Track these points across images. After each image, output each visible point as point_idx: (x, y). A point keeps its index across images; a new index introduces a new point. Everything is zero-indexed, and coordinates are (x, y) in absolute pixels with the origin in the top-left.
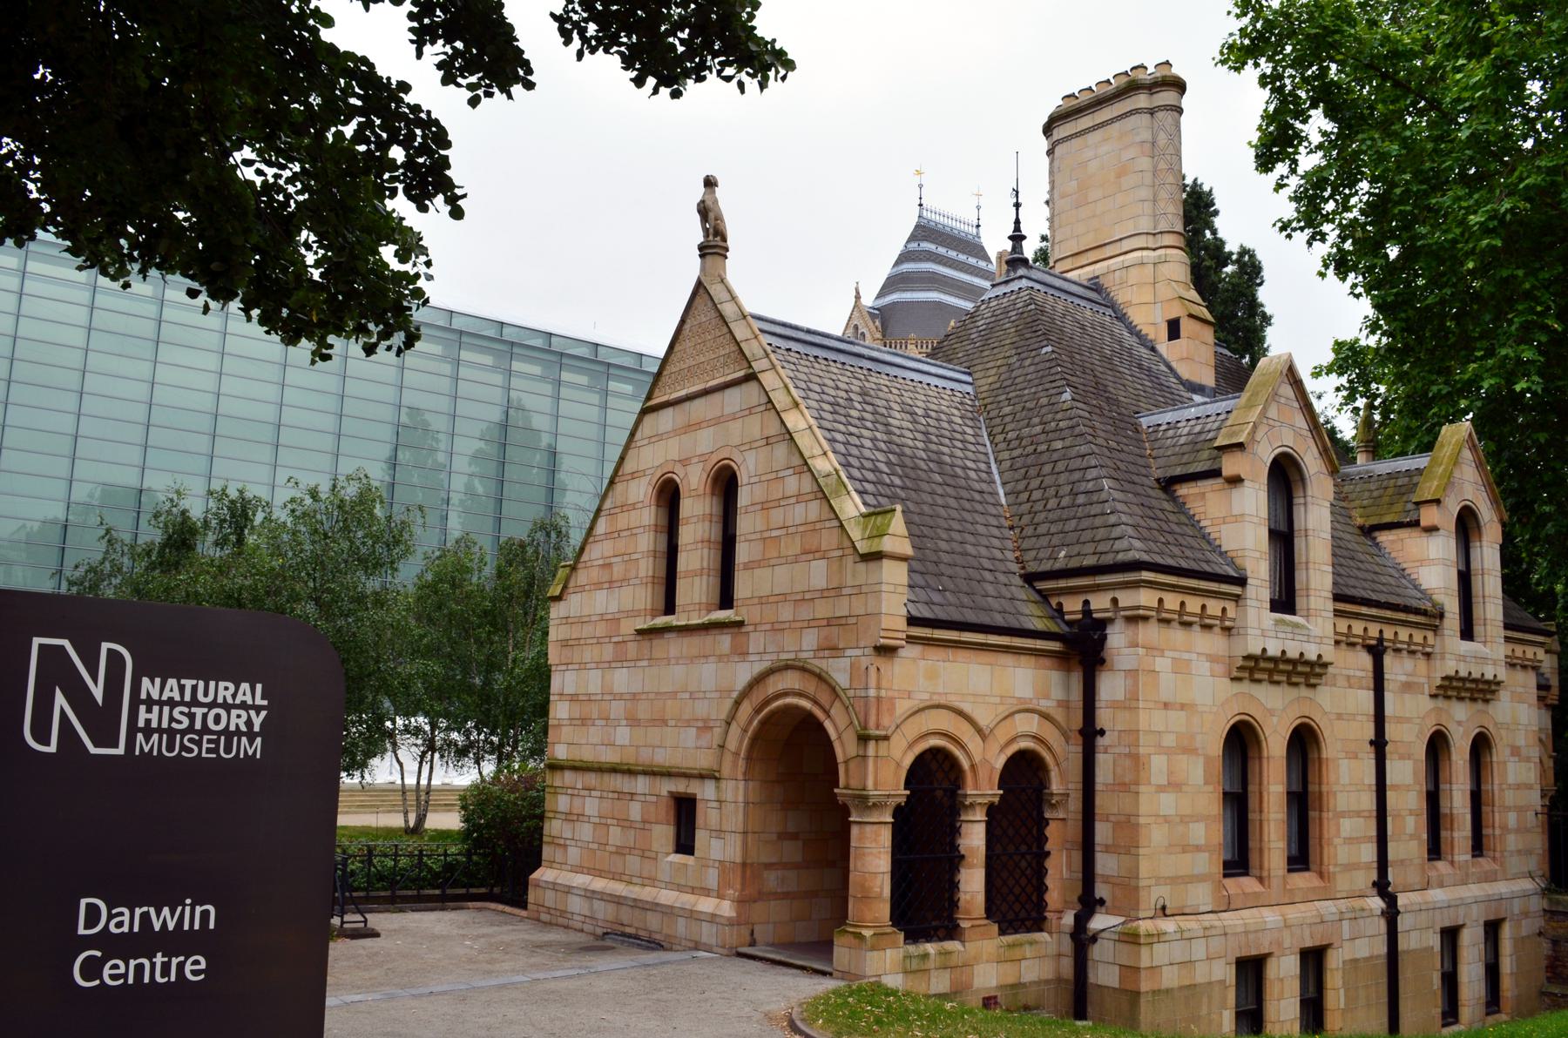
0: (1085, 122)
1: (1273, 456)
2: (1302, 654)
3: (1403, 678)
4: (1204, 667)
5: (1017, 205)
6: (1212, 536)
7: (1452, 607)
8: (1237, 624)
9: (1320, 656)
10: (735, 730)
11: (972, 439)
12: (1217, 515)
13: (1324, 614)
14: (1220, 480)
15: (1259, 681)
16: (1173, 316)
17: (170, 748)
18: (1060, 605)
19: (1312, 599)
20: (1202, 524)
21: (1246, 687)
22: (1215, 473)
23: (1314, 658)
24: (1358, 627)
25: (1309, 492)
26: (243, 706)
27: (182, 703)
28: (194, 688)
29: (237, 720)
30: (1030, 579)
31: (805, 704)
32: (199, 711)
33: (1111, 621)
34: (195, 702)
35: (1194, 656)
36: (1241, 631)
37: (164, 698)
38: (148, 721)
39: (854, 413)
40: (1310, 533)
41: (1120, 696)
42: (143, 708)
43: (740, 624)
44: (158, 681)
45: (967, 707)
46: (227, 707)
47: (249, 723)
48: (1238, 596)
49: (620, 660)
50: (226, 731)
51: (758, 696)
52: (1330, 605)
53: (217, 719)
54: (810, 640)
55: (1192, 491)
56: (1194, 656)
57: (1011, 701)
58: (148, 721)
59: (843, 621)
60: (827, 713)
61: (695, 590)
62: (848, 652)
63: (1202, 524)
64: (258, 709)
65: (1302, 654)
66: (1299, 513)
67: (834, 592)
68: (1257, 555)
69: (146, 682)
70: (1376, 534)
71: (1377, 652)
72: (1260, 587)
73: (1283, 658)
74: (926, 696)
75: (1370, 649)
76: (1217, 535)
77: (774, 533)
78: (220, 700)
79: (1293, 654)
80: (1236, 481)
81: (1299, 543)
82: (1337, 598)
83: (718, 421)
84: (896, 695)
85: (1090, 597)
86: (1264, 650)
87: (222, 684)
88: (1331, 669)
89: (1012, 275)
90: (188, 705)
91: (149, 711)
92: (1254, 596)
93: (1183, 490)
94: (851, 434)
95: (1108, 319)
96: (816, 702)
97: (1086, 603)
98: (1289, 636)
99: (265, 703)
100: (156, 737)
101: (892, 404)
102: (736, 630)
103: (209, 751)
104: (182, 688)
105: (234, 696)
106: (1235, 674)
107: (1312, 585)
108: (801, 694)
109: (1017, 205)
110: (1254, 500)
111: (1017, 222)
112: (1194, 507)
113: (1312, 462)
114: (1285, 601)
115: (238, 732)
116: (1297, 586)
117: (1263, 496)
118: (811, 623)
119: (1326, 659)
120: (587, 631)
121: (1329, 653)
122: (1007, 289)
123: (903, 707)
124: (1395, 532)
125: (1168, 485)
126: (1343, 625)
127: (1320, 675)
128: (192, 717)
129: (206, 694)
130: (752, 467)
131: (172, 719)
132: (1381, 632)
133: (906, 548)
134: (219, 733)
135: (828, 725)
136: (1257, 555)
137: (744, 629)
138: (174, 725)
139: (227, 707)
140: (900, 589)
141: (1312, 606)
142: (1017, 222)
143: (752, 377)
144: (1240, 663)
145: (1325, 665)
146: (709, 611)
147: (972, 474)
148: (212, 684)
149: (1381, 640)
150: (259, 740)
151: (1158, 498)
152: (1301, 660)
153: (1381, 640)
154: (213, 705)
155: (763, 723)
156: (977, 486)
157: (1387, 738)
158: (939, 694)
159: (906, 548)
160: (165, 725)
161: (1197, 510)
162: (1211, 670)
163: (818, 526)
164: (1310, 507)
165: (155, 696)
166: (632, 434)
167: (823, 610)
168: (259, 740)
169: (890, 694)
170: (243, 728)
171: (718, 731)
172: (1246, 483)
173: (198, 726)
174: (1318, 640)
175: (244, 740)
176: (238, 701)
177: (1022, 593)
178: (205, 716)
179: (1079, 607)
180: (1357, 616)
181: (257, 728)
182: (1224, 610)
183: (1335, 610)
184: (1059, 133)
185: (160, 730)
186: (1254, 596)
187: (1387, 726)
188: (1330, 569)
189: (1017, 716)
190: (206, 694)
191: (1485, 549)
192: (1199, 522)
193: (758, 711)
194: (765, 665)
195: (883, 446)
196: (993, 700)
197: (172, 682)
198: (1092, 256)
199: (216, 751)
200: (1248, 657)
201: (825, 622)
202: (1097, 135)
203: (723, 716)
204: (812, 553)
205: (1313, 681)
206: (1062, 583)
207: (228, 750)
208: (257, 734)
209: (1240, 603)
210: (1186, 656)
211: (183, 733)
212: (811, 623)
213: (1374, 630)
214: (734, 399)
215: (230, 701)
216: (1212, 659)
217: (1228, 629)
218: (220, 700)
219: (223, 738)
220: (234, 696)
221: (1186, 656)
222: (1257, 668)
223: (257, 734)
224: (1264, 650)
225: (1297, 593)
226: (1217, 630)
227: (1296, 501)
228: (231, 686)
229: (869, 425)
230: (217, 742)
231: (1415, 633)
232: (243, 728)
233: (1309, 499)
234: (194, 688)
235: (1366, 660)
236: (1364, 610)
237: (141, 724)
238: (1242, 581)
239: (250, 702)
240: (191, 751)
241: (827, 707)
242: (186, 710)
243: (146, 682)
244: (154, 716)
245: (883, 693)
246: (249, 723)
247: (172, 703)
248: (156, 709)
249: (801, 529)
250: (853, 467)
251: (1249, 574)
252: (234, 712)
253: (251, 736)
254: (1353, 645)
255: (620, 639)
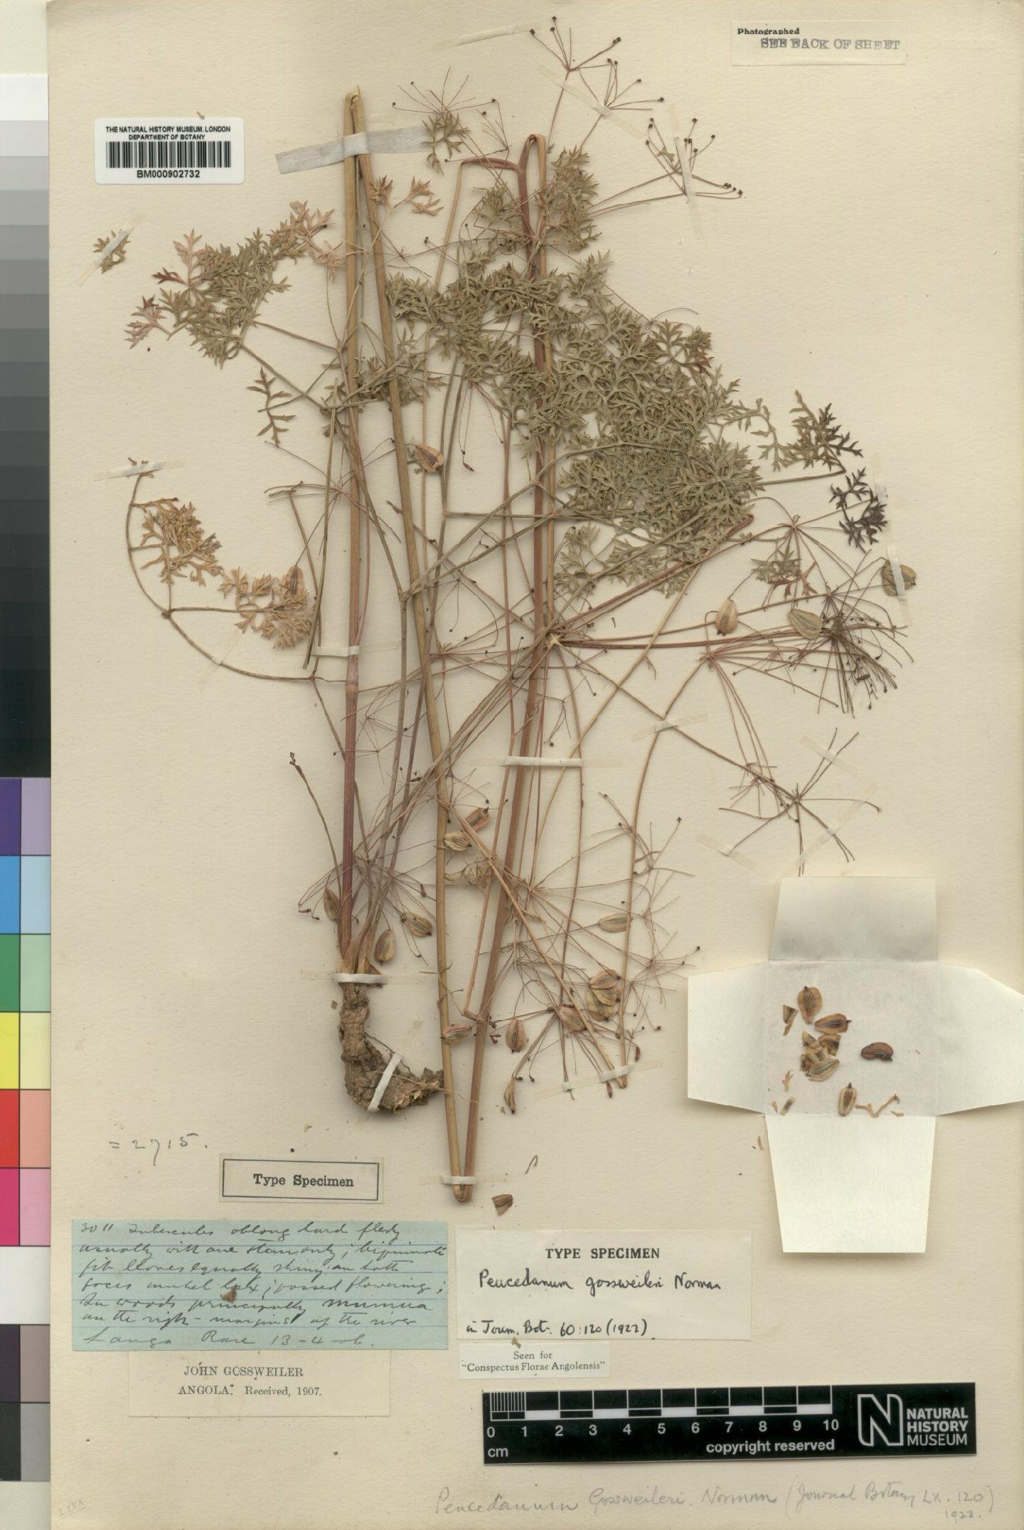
17: (924, 1442)
26: (956, 1419)
27: (927, 1420)
28: (932, 1413)
29: (953, 1426)
32: (935, 1423)
34: (933, 1419)
37: (919, 1418)
38: (912, 1430)
42: (909, 1424)
44: (915, 1410)
46: (948, 1420)
47: (959, 1427)
50: (949, 1432)
53: (944, 1426)
58: (912, 1430)
64: (963, 1420)
69: (909, 1411)
78: (944, 1417)
87: (945, 1409)
90: (930, 1420)
91: (912, 1425)
99: (967, 1417)
100: (916, 1436)
103: (942, 1442)
104: (926, 1413)
105: (951, 1414)
115: (955, 1432)
128: (932, 1426)
129: (938, 1415)
131: (923, 1428)
134: (946, 1433)
138: (924, 1430)
139: (948, 1420)
148: (940, 1409)
150: (965, 1436)
154: (941, 1419)
160: (920, 1430)
165: (914, 1417)
168: (965, 1436)
170: (957, 1430)
173: (936, 1430)
175: (958, 1435)
176: (953, 1417)
178: (938, 1425)
181: (964, 1429)
185: (918, 1433)
190: (938, 1415)
197: (921, 1410)
199: (945, 1442)
207: (951, 1440)
208: (964, 1432)
211: (929, 1434)
215: (949, 1417)
218: (944, 1417)
219: (948, 1436)
220: (951, 1414)
223: (964, 1432)
228: (949, 1410)
230: (945, 1437)
232: (957, 1430)
234: (932, 1413)
237: (909, 1431)
239: (959, 1417)
240: (933, 1442)
242: (929, 1423)
243: (909, 1411)
244: (915, 1427)
246: (959, 1427)
247: (922, 1420)
248: (915, 1423)
252: (952, 1423)
253: (961, 1434)
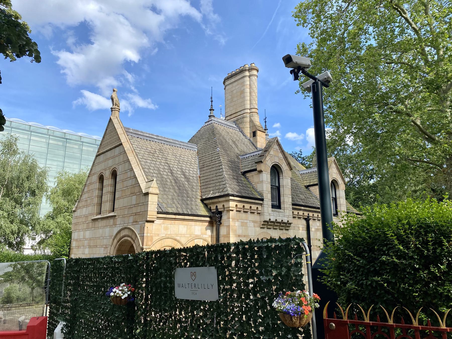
0: (233, 80)
1: (272, 165)
2: (282, 220)
3: (317, 227)
4: (252, 224)
5: (212, 101)
6: (255, 187)
7: (267, 196)
8: (262, 212)
9: (288, 221)
10: (113, 247)
11: (194, 163)
12: (256, 181)
13: (289, 209)
14: (257, 172)
15: (270, 228)
16: (254, 130)
18: (210, 207)
19: (285, 205)
20: (253, 184)
21: (265, 230)
22: (255, 170)
23: (286, 221)
24: (301, 213)
25: (284, 175)
30: (202, 200)
31: (129, 239)
33: (223, 211)
35: (248, 221)
36: (263, 214)
39: (156, 155)
40: (284, 186)
41: (225, 234)
43: (115, 216)
45: (178, 238)
48: (262, 204)
49: (88, 229)
51: (118, 237)
52: (291, 207)
54: (131, 219)
55: (250, 175)
56: (248, 221)
57: (193, 236)
59: (139, 213)
60: (134, 241)
61: (107, 206)
62: (140, 223)
63: (253, 184)
65: (282, 220)
66: (281, 180)
67: (137, 205)
68: (267, 192)
70: (309, 188)
71: (307, 220)
72: (268, 201)
73: (276, 221)
74: (164, 235)
75: (305, 219)
76: (256, 187)
77: (124, 189)
79: (279, 220)
80: (261, 172)
81: (281, 189)
82: (293, 205)
83: (113, 157)
84: (154, 235)
85: (218, 205)
86: (270, 219)
88: (292, 225)
89: (210, 120)
92: (266, 204)
93: (248, 175)
94: (153, 161)
95: (237, 132)
96: (132, 239)
97: (217, 206)
98: (278, 215)
101: (169, 153)
102: (114, 218)
106: (261, 226)
107: (285, 201)
108: (128, 236)
109: (212, 101)
110: (266, 177)
111: (212, 106)
112: (251, 179)
113: (284, 167)
114: (277, 206)
116: (281, 201)
117: (269, 176)
118: (132, 215)
119: (290, 222)
120: (80, 220)
121: (291, 220)
122: (208, 123)
123: (155, 238)
124: (314, 187)
125: (244, 173)
126: (296, 212)
127: (289, 227)
130: (120, 170)
132: (308, 214)
133: (157, 191)
135: (134, 245)
136: (267, 192)
137: (116, 217)
140: (155, 203)
141: (285, 207)
142: (212, 106)
143: (121, 144)
144: (263, 223)
145: (290, 224)
146: (109, 213)
147: (191, 172)
149: (308, 217)
151: (243, 178)
152: (282, 222)
153: (308, 217)
155: (120, 245)
156: (192, 175)
157: (311, 244)
158: (169, 234)
159: (157, 191)
161: (252, 180)
162: (254, 225)
163: (135, 186)
164: (284, 179)
166: (94, 163)
167: (134, 210)
169: (151, 235)
171: (109, 248)
172: (263, 172)
174: (287, 216)
177: (201, 205)
179: (215, 208)
180: (300, 210)
182: (257, 208)
183: (292, 208)
184: (227, 83)
186: (266, 204)
187: (311, 241)
188: (291, 196)
189: (195, 240)
191: (340, 191)
192: (252, 183)
193: (118, 242)
194: (121, 228)
195: (163, 164)
196: (187, 236)
198: (234, 115)
200: (264, 221)
201: (135, 214)
202: (236, 83)
203: (110, 244)
204: (133, 194)
205: (287, 228)
206: (211, 201)
209: (262, 206)
210: (245, 221)
212: (132, 215)
213: (306, 214)
214: (117, 150)
216: (254, 222)
217: (259, 213)
221: (245, 221)
222: (268, 224)
224: (270, 219)
225: (281, 203)
226: (256, 214)
227: (280, 177)
229: (160, 158)
231: (314, 214)
233: (284, 177)
235: (304, 222)
236: (302, 208)
238: (262, 200)
241: (134, 239)
245: (149, 235)
249: (131, 187)
250: (151, 169)
251: (264, 197)
254: (300, 218)
255: (88, 222)
